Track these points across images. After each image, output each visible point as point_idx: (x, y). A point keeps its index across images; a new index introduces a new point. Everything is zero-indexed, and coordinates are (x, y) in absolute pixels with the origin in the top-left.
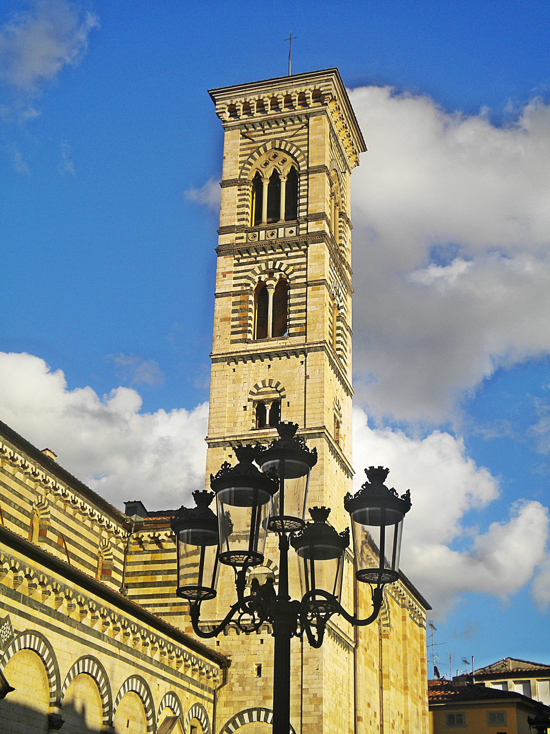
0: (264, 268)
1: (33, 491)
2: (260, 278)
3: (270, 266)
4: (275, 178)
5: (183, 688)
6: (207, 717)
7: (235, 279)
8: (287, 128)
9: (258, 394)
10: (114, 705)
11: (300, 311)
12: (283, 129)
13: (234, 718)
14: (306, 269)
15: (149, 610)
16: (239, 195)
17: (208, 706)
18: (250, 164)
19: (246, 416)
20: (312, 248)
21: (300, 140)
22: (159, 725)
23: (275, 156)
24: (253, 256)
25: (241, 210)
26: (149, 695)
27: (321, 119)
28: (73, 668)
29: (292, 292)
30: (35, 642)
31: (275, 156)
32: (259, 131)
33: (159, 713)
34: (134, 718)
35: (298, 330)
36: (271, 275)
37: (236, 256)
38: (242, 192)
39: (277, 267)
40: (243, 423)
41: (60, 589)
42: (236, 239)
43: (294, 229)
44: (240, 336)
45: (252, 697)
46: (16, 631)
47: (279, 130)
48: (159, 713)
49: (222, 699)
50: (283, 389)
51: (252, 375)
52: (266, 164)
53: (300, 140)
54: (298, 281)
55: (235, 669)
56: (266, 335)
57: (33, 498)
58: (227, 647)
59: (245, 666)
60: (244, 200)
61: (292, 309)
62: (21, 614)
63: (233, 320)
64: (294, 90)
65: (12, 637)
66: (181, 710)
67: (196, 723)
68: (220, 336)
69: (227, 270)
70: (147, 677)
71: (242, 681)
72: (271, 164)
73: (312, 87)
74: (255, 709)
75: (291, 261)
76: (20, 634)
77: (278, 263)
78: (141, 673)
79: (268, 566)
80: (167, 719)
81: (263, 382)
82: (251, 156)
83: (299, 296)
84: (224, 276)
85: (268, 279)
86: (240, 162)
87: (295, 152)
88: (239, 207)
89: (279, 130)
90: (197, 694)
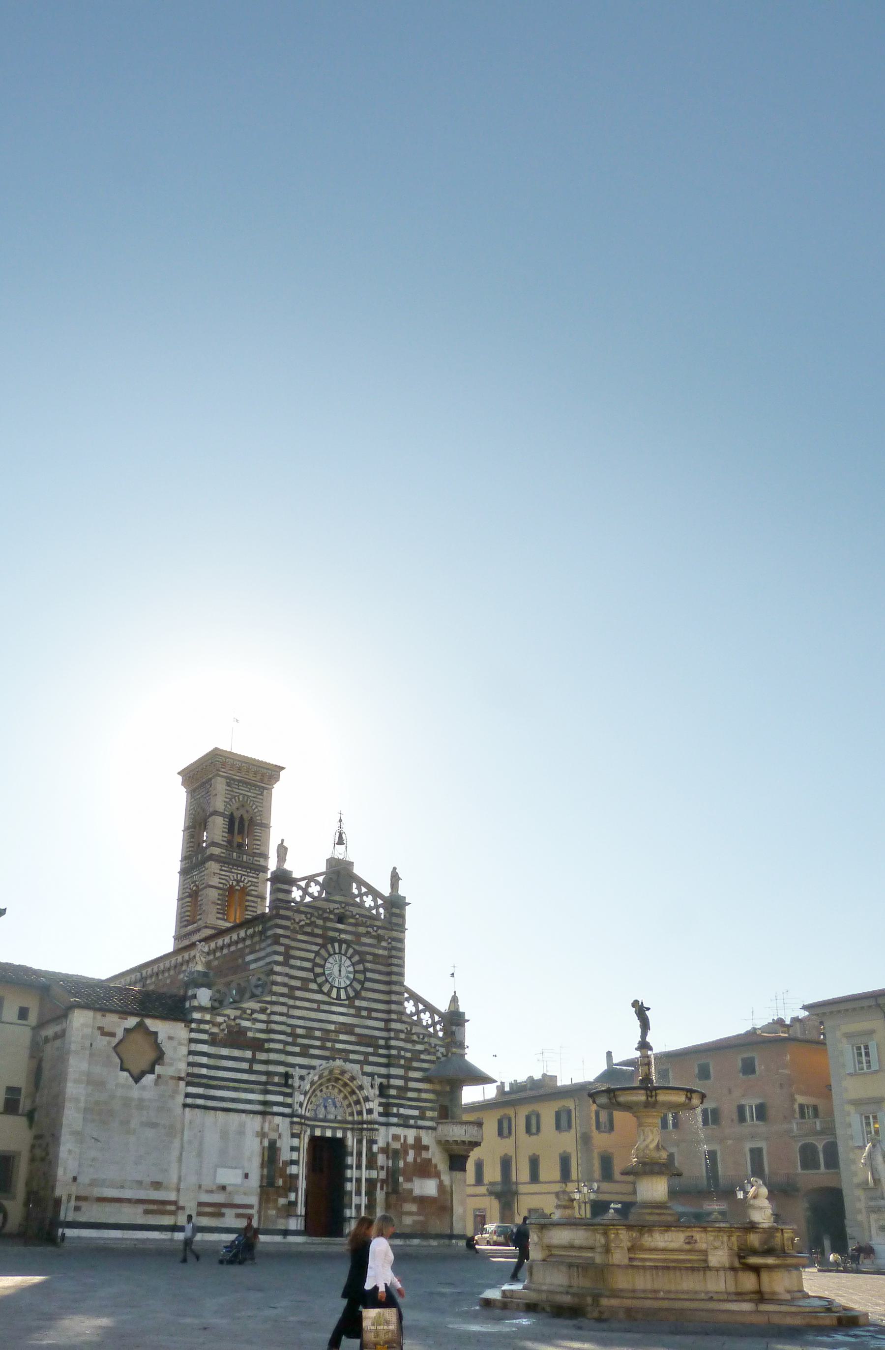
2: (232, 883)
3: (239, 878)
8: (251, 791)
12: (249, 790)
16: (223, 824)
18: (230, 805)
21: (258, 802)
23: (243, 806)
24: (230, 868)
31: (243, 806)
32: (236, 785)
37: (221, 864)
39: (243, 880)
43: (251, 858)
47: (246, 789)
53: (258, 802)
54: (253, 892)
60: (226, 828)
64: (260, 769)
75: (250, 879)
82: (231, 800)
83: (253, 902)
84: (214, 875)
86: (225, 802)
89: (246, 789)
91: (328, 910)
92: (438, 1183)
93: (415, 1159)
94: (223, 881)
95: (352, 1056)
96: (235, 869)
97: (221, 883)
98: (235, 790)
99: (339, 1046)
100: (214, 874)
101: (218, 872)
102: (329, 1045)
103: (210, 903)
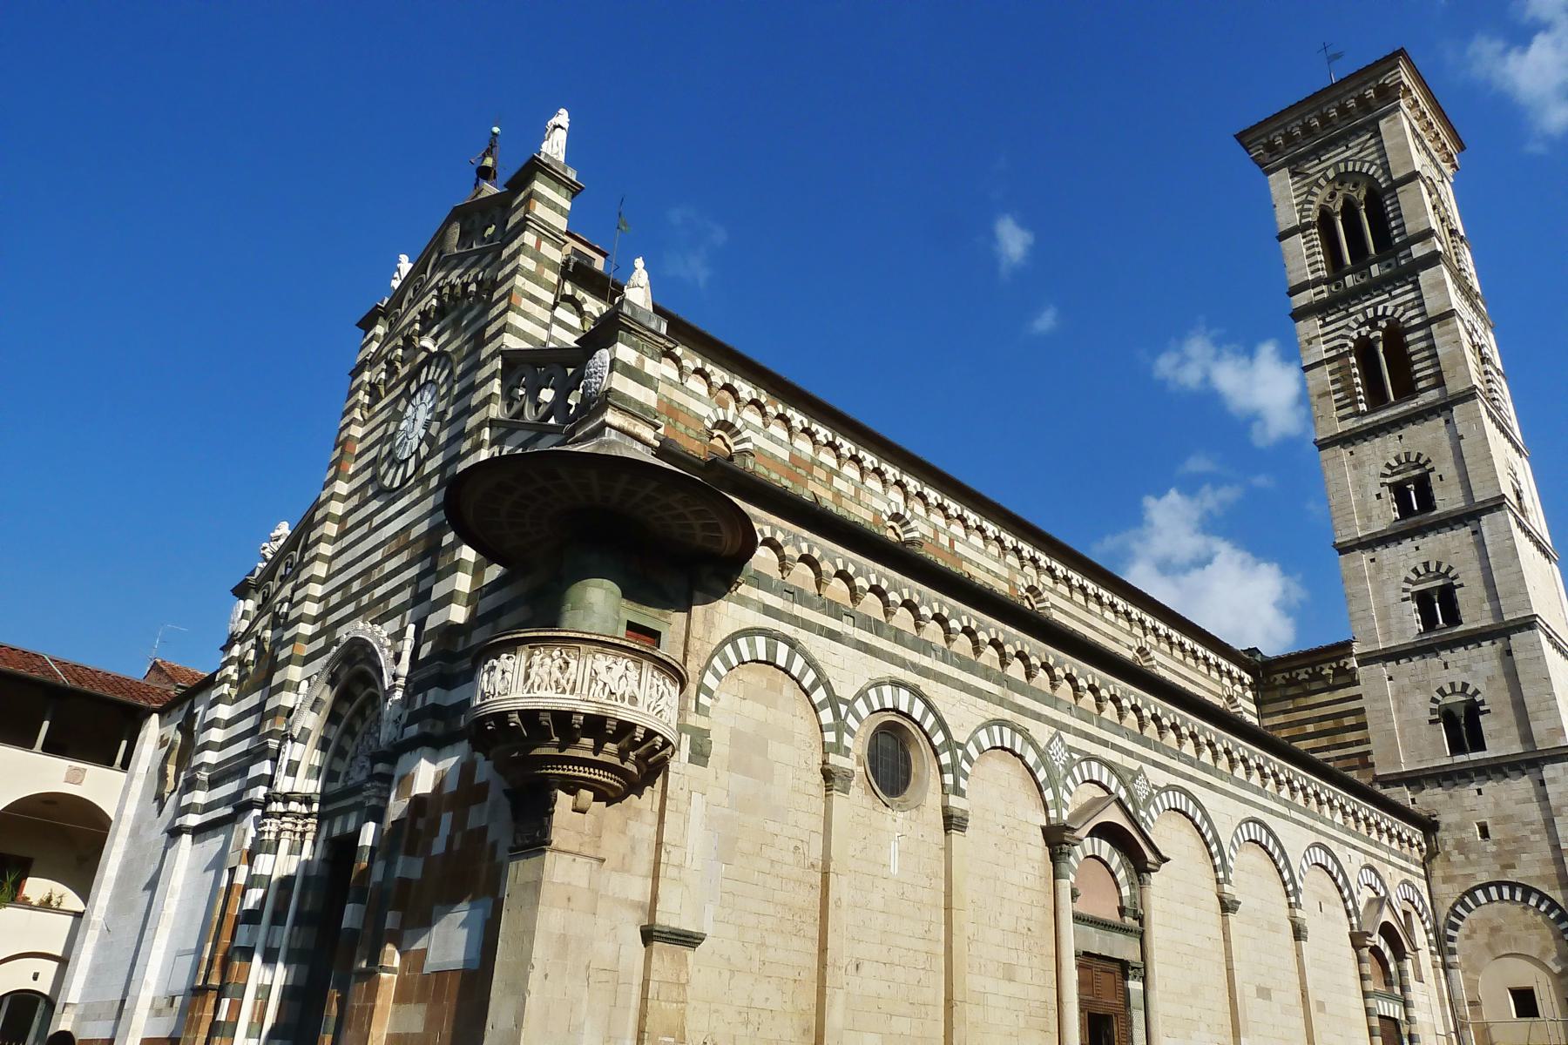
0: (1361, 319)
1: (1130, 633)
4: (1349, 210)
5: (1382, 859)
6: (1421, 899)
7: (1324, 343)
8: (1350, 145)
9: (1393, 474)
10: (1299, 884)
11: (1426, 359)
12: (1344, 148)
13: (1462, 898)
14: (1423, 304)
15: (1317, 756)
16: (1304, 244)
17: (1421, 885)
18: (1311, 202)
19: (1382, 505)
20: (1424, 277)
22: (1361, 908)
25: (1312, 260)
26: (1340, 869)
27: (1395, 118)
28: (1236, 834)
29: (1409, 337)
30: (1181, 801)
31: (1341, 184)
32: (1315, 159)
33: (1359, 893)
34: (1328, 901)
35: (1431, 381)
36: (1374, 326)
38: (1309, 238)
39: (1380, 313)
40: (1381, 516)
41: (1198, 732)
42: (1315, 295)
43: (1392, 261)
44: (1349, 410)
45: (1483, 868)
46: (1155, 787)
48: (1359, 893)
49: (1438, 873)
50: (1429, 461)
51: (1378, 453)
52: (1333, 196)
55: (1447, 833)
56: (1386, 398)
57: (1132, 642)
58: (1428, 804)
59: (1462, 827)
60: (1313, 246)
61: (1414, 358)
62: (1156, 764)
63: (1335, 392)
65: (1151, 794)
66: (1385, 888)
67: (1409, 908)
68: (1322, 416)
69: (1312, 335)
70: (1333, 846)
71: (1461, 846)
72: (1339, 194)
73: (1372, 84)
74: (1491, 884)
76: (1161, 790)
77: (1380, 308)
78: (1324, 840)
79: (1463, 692)
80: (1370, 901)
81: (1397, 459)
82: (1310, 193)
85: (1370, 332)
87: (1369, 170)
88: (1308, 257)
90: (1402, 868)
91: (418, 317)
92: (489, 916)
93: (450, 840)
94: (1336, 343)
95: (395, 602)
96: (1356, 305)
97: (1332, 349)
98: (1310, 172)
99: (379, 592)
100: (1309, 342)
101: (1320, 332)
102: (365, 599)
103: (1315, 399)
